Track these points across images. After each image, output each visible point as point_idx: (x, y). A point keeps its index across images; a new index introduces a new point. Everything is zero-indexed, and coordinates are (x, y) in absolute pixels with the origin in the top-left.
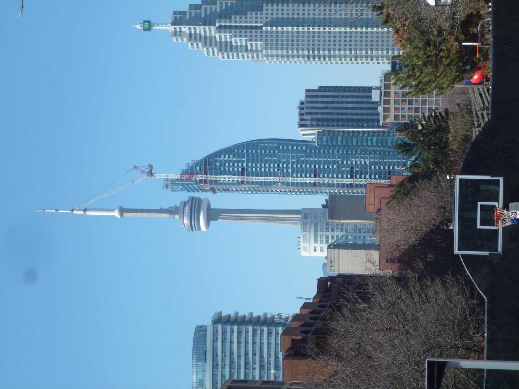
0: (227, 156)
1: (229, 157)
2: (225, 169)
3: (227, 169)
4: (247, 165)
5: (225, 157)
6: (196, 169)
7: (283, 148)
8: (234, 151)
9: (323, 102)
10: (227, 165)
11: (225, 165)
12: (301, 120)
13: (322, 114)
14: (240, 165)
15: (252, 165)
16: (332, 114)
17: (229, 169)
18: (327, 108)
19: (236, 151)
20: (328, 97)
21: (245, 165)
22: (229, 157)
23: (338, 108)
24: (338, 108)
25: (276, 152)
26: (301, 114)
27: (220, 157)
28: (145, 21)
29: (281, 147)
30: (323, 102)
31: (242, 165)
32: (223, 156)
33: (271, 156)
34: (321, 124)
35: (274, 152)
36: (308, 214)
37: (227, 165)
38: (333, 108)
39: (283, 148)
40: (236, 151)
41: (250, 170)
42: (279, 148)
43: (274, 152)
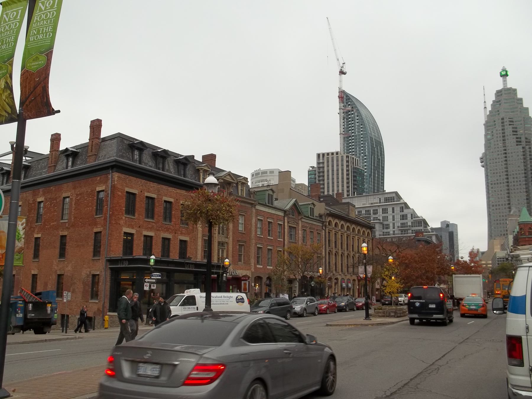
0: (358, 121)
1: (357, 122)
2: (350, 121)
3: (350, 123)
4: (353, 136)
5: (357, 119)
6: (349, 102)
7: (365, 159)
8: (362, 125)
9: (338, 170)
10: (353, 122)
11: (352, 121)
12: (323, 155)
13: (328, 171)
14: (353, 131)
15: (353, 139)
16: (328, 179)
17: (350, 124)
18: (333, 175)
19: (362, 126)
20: (343, 174)
21: (353, 134)
22: (357, 122)
23: (333, 183)
24: (333, 183)
25: (362, 155)
26: (328, 154)
27: (357, 116)
28: (506, 72)
29: (365, 157)
30: (338, 170)
31: (353, 133)
32: (358, 118)
33: (360, 151)
34: (320, 170)
35: (362, 153)
36: (273, 174)
37: (353, 122)
38: (333, 179)
39: (365, 159)
40: (362, 126)
41: (350, 138)
42: (365, 156)
43: (362, 153)
